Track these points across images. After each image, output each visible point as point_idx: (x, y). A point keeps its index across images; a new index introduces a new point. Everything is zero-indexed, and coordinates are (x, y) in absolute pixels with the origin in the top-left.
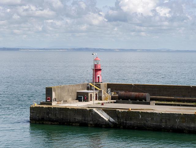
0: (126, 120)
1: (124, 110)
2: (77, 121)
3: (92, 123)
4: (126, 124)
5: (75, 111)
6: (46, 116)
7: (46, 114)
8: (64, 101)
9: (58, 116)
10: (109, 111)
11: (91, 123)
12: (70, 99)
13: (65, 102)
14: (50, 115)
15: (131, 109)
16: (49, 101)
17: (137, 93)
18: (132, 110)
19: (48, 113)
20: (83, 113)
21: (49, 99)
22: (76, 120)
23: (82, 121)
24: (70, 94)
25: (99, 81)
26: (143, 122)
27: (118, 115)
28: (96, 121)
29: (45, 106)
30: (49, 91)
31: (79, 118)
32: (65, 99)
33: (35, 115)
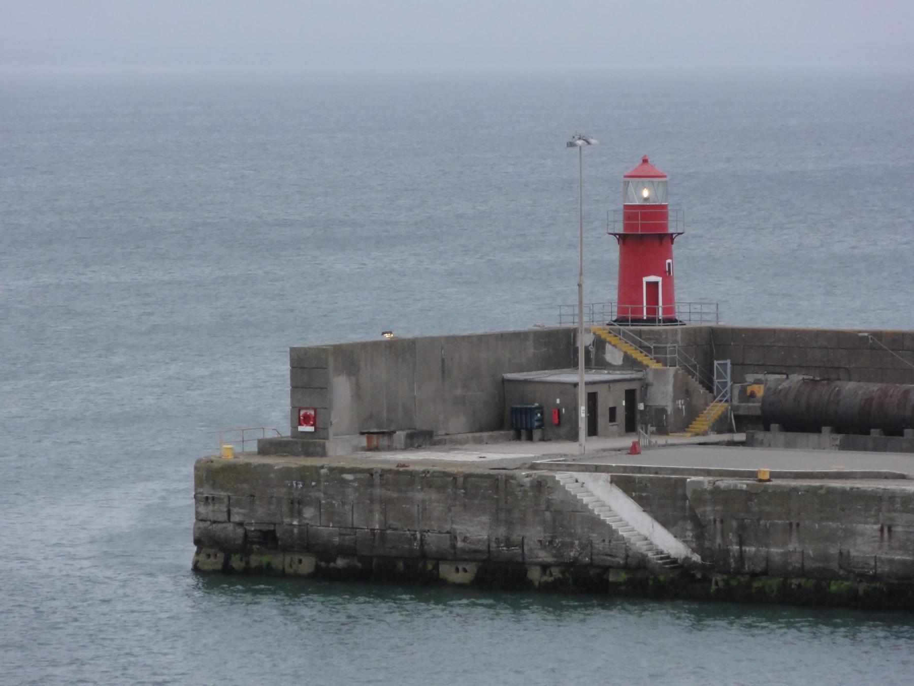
0: (740, 537)
1: (793, 483)
2: (463, 551)
3: (550, 560)
4: (743, 565)
5: (450, 491)
6: (287, 520)
7: (285, 509)
8: (410, 437)
9: (357, 519)
10: (644, 489)
11: (545, 556)
12: (457, 423)
13: (421, 438)
14: (309, 513)
15: (774, 475)
16: (311, 429)
17: (874, 388)
18: (776, 482)
19: (296, 505)
20: (497, 500)
21: (306, 420)
22: (460, 544)
23: (493, 545)
24: (459, 392)
25: (652, 311)
26: (833, 550)
27: (699, 511)
28: (572, 545)
29: (277, 462)
30: (645, 239)
31: (476, 529)
32: (421, 424)
33: (225, 517)
